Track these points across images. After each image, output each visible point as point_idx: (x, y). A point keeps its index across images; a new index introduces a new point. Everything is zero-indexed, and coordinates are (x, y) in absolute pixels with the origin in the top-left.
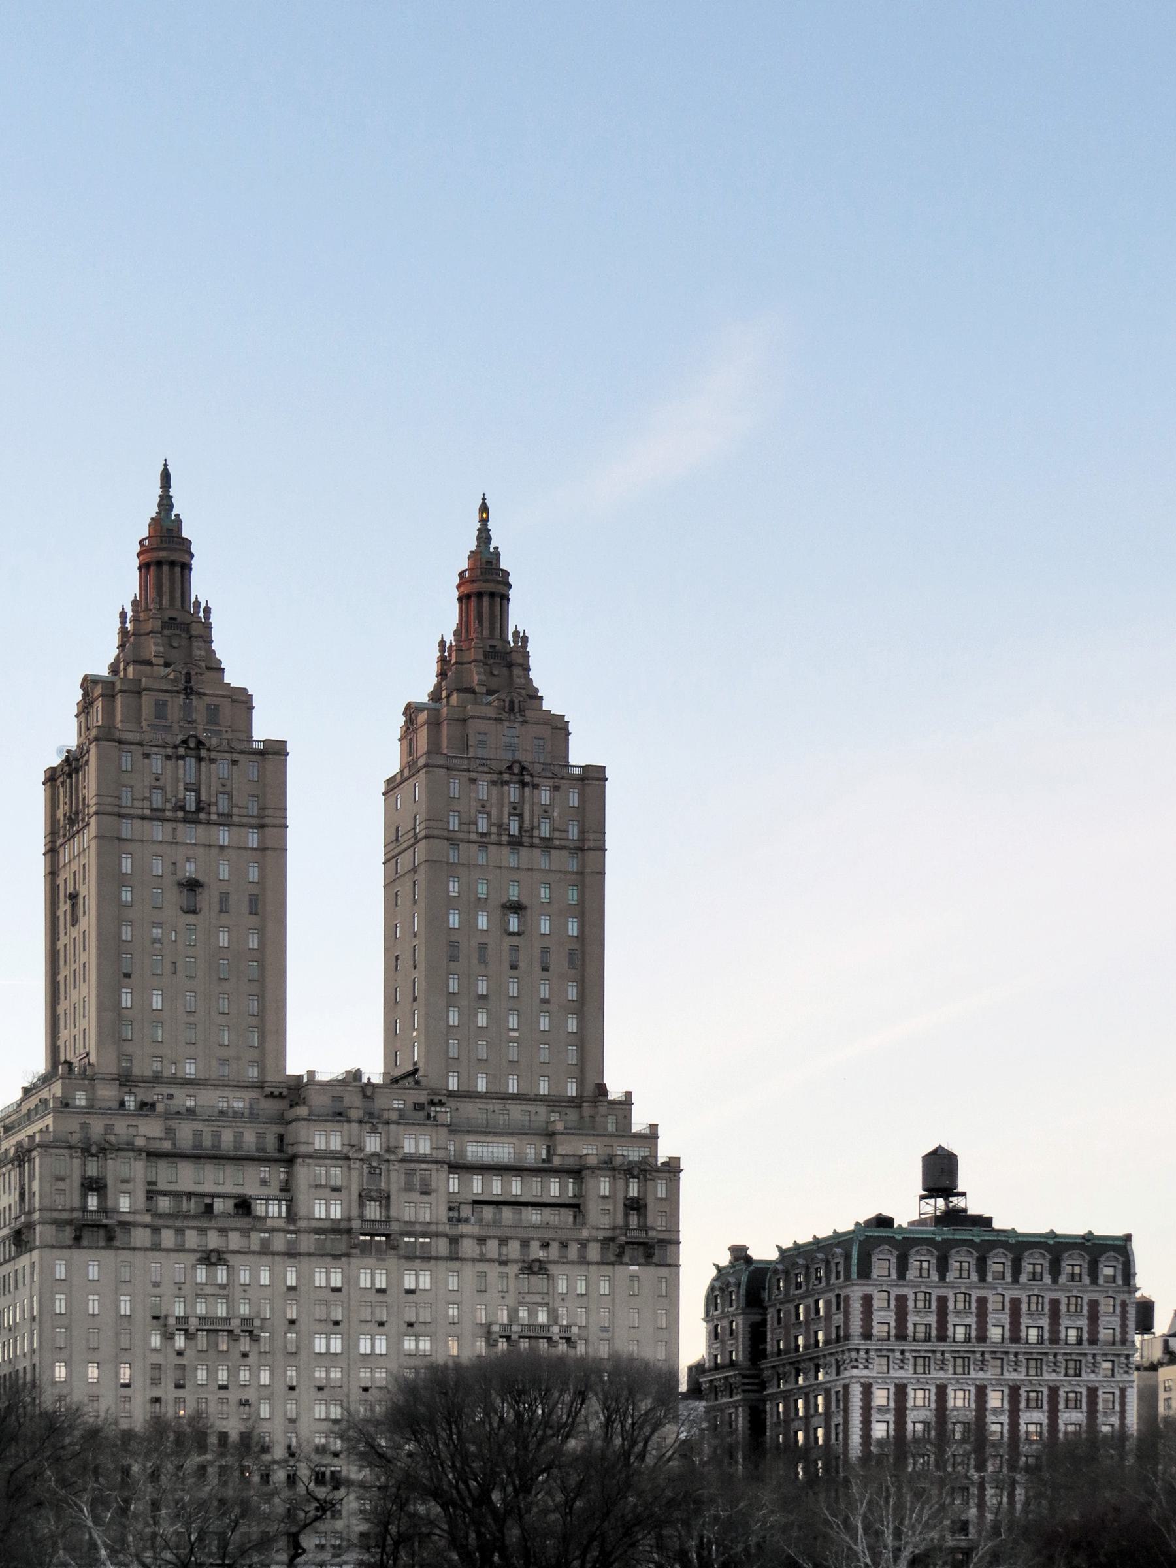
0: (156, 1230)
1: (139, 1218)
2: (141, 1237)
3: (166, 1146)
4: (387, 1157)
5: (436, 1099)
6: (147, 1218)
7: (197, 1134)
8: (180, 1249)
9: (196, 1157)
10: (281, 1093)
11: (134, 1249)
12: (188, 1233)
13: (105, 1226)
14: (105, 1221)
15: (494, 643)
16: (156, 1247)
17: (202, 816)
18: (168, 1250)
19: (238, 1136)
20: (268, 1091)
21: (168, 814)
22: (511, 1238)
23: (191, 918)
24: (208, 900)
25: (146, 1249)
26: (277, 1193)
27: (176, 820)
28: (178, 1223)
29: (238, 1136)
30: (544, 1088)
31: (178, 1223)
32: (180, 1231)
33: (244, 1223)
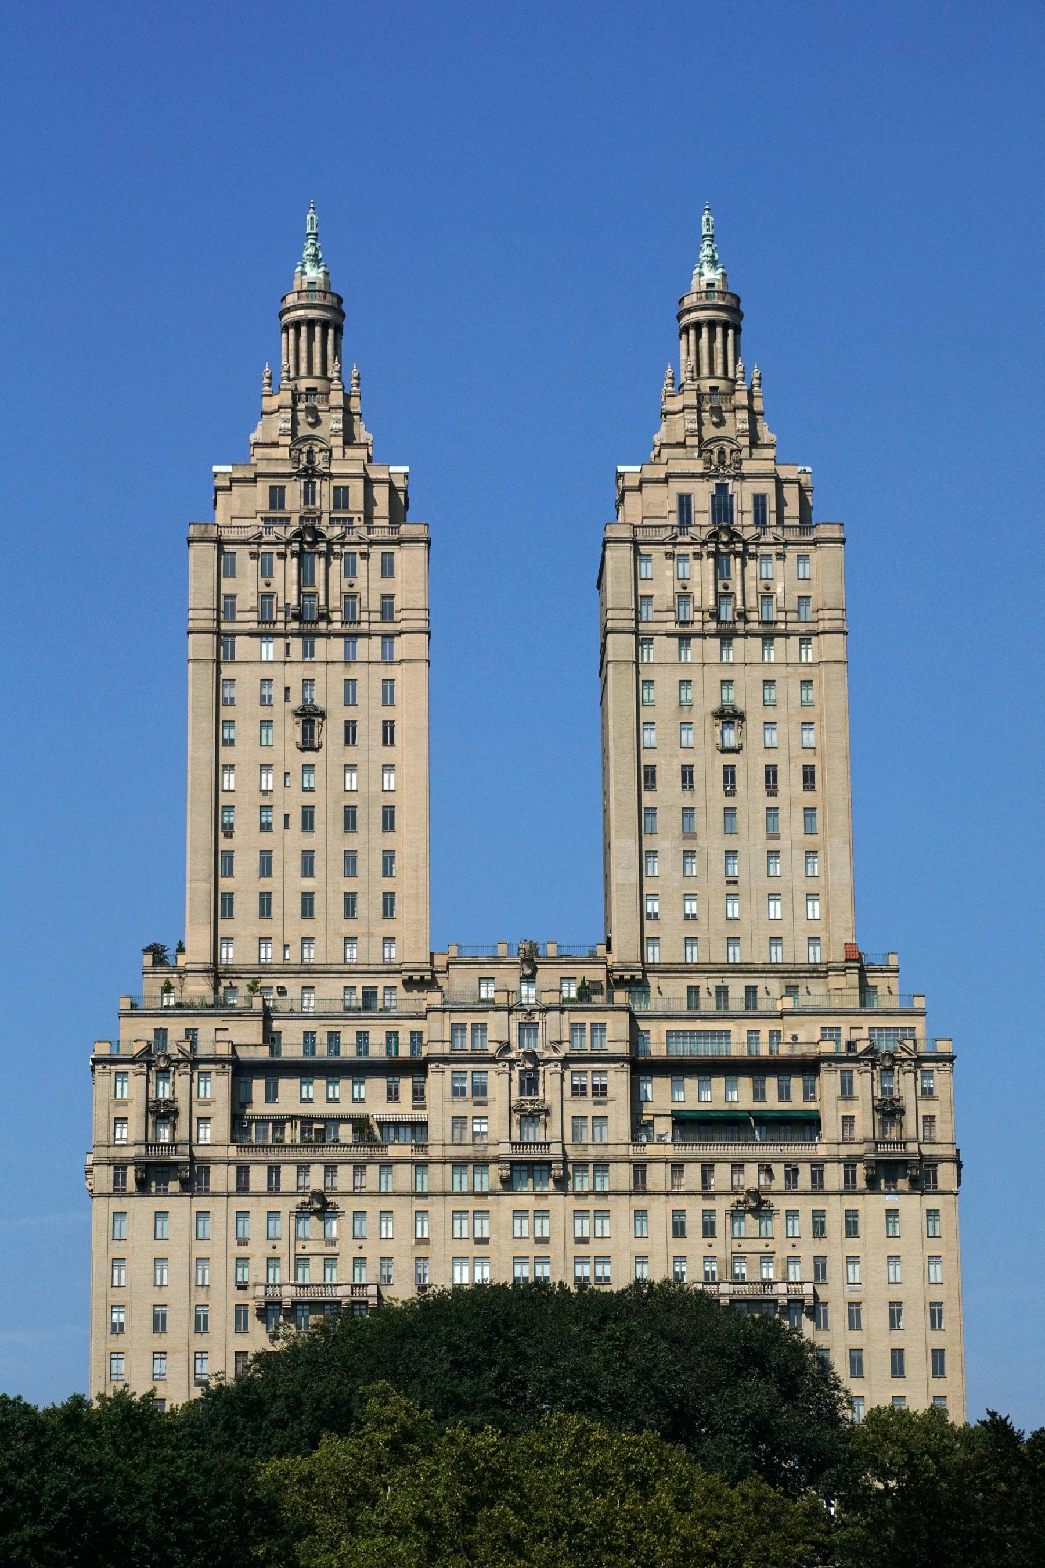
0: (243, 1169)
1: (220, 1152)
2: (221, 1178)
3: (263, 1053)
4: (548, 1055)
5: (627, 975)
6: (233, 1152)
7: (309, 1036)
8: (273, 1189)
9: (304, 1070)
10: (422, 977)
11: (215, 1195)
12: (284, 1168)
13: (176, 1164)
14: (174, 1158)
15: (713, 383)
16: (243, 1189)
17: (322, 625)
18: (258, 1195)
19: (362, 1037)
20: (406, 975)
21: (280, 626)
22: (719, 1161)
23: (309, 757)
24: (331, 732)
25: (229, 1195)
26: (410, 1110)
27: (285, 635)
28: (273, 1156)
29: (362, 1037)
30: (778, 955)
31: (273, 1156)
32: (274, 1169)
33: (361, 1153)
